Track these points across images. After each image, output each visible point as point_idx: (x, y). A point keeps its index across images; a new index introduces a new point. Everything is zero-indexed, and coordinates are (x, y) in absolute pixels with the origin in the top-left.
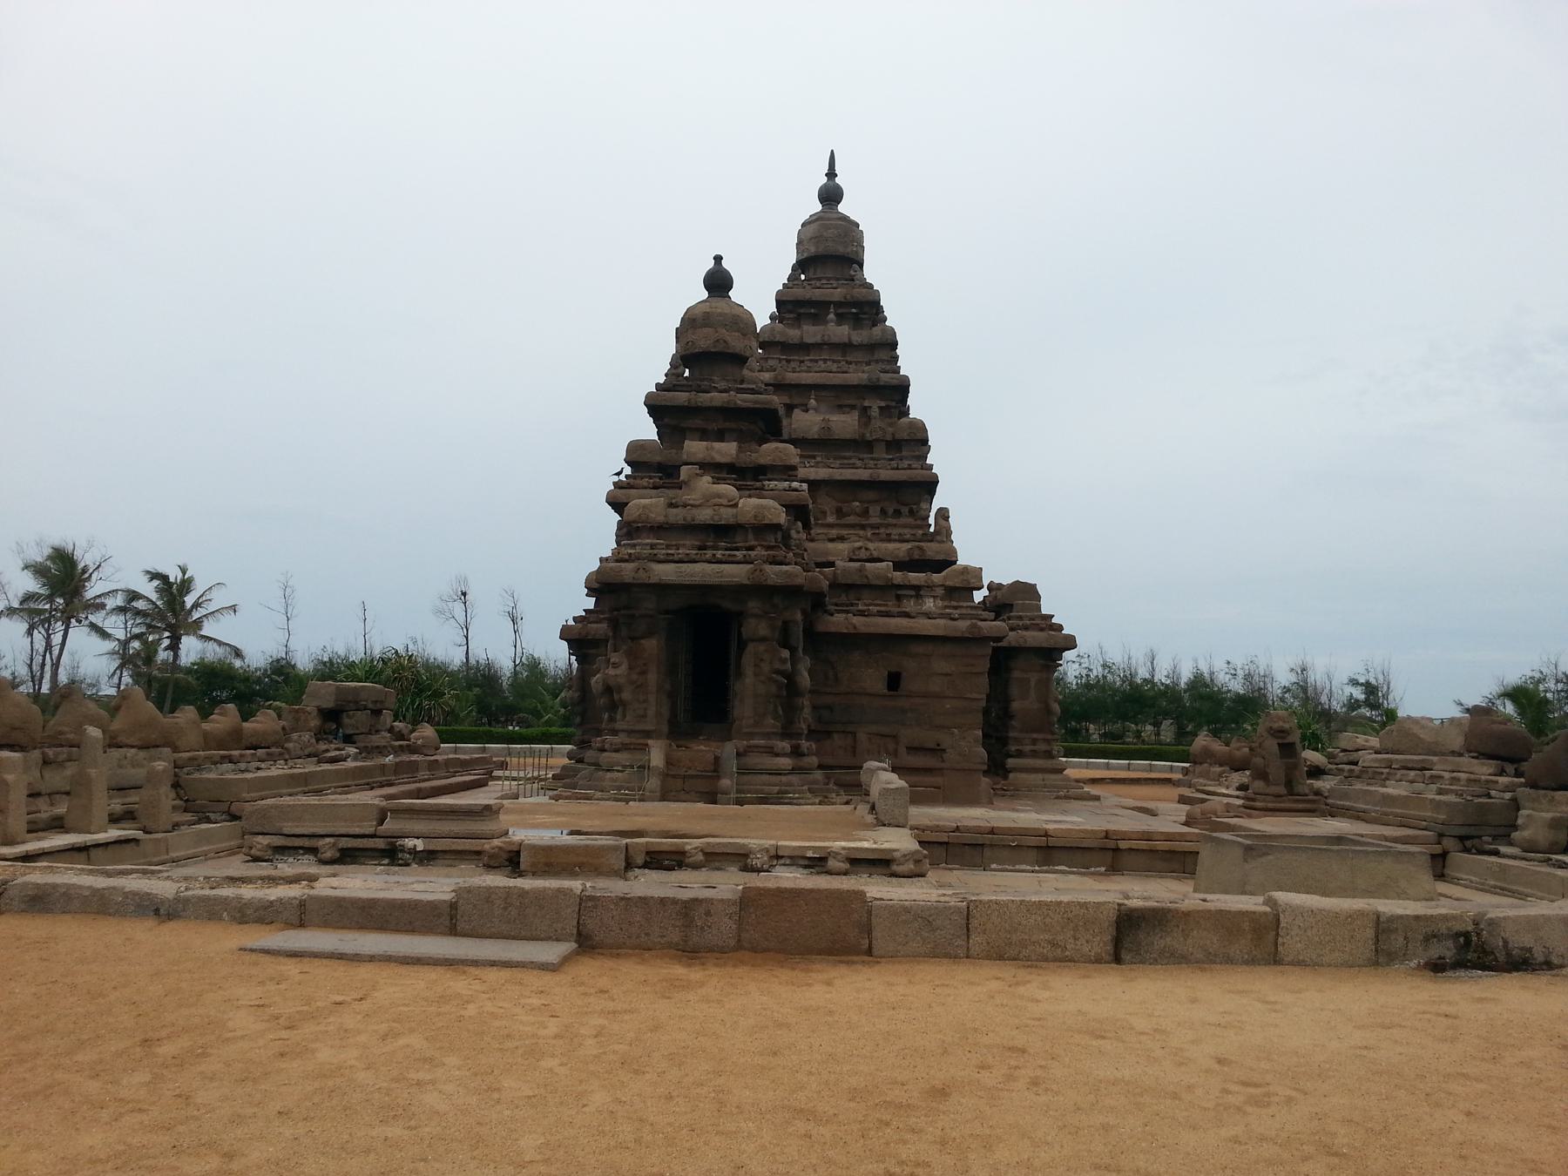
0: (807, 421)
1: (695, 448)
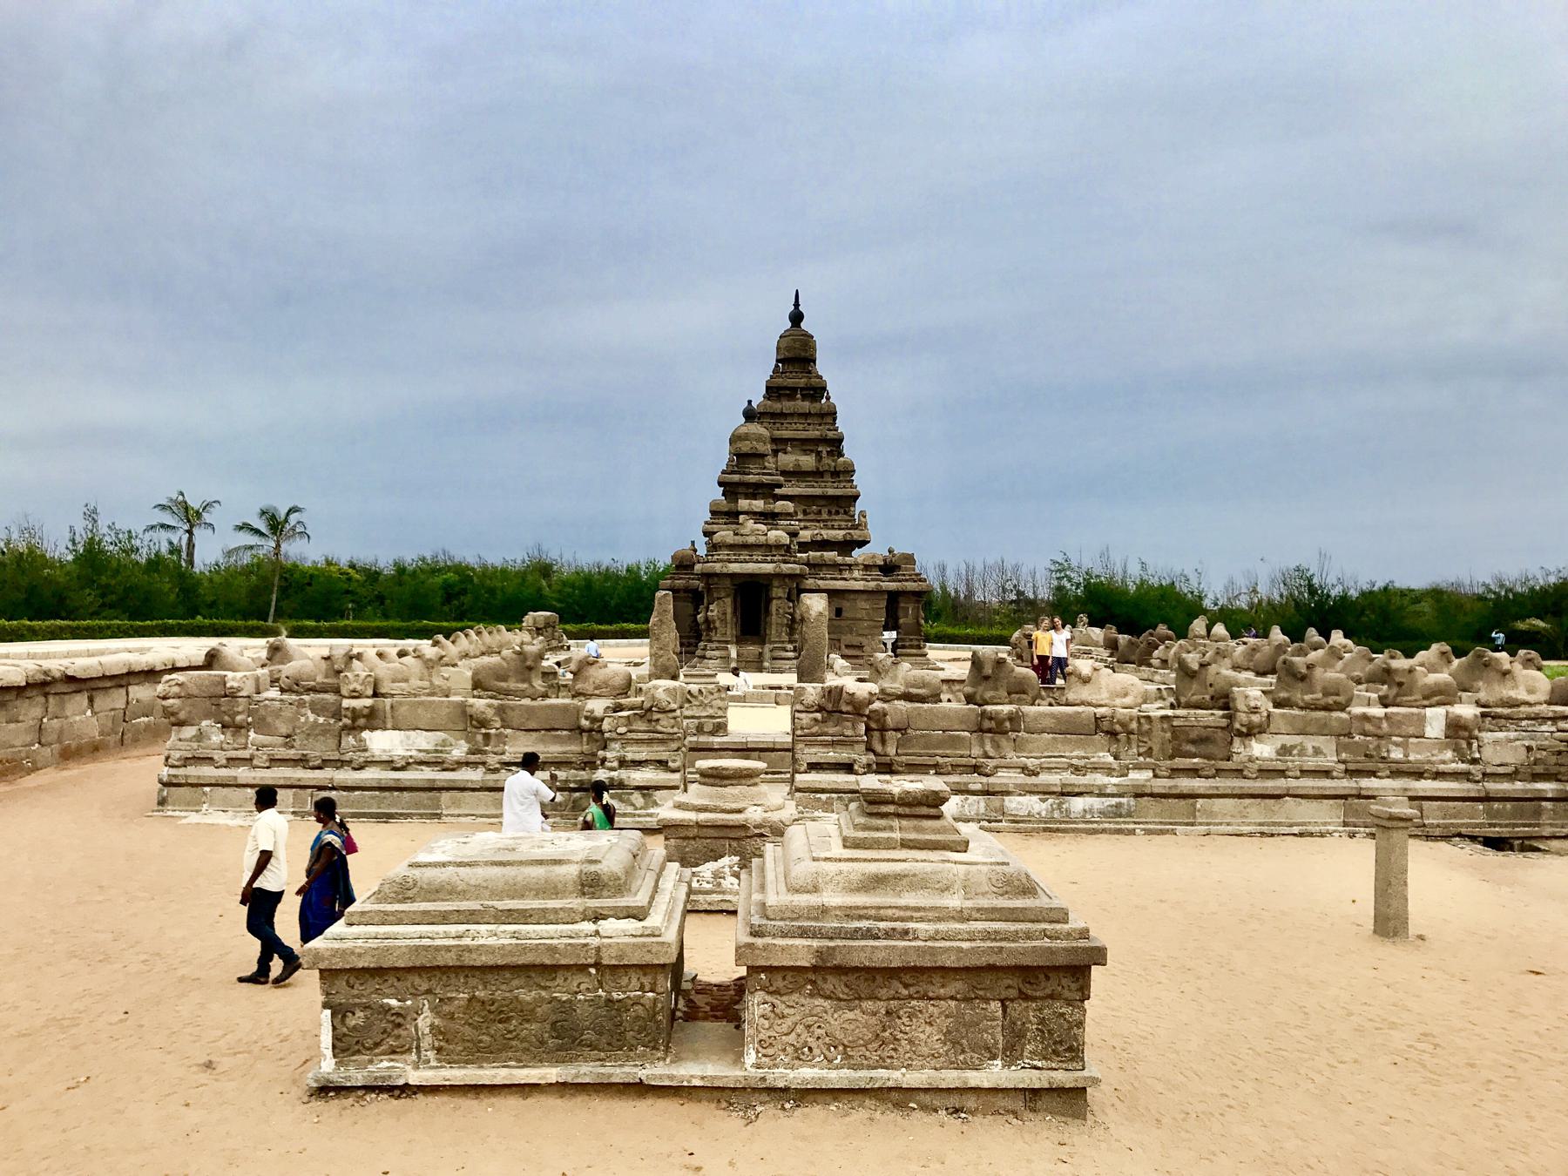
0: (788, 460)
1: (743, 504)
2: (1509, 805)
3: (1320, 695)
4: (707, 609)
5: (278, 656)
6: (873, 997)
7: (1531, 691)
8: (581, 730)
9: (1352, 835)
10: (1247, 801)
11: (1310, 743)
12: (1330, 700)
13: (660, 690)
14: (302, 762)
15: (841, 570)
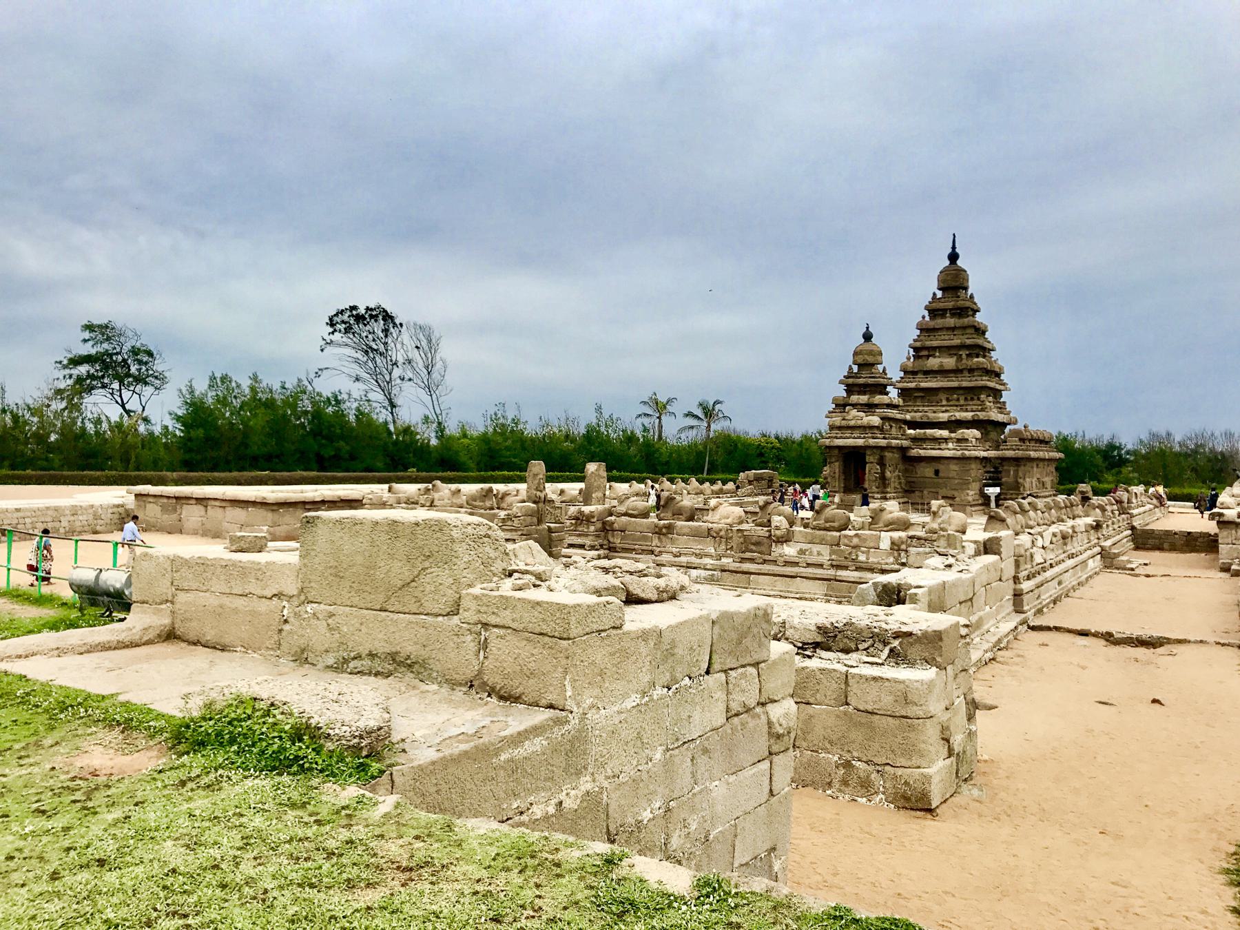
1: (855, 398)
9: (828, 601)
11: (816, 548)
12: (828, 525)
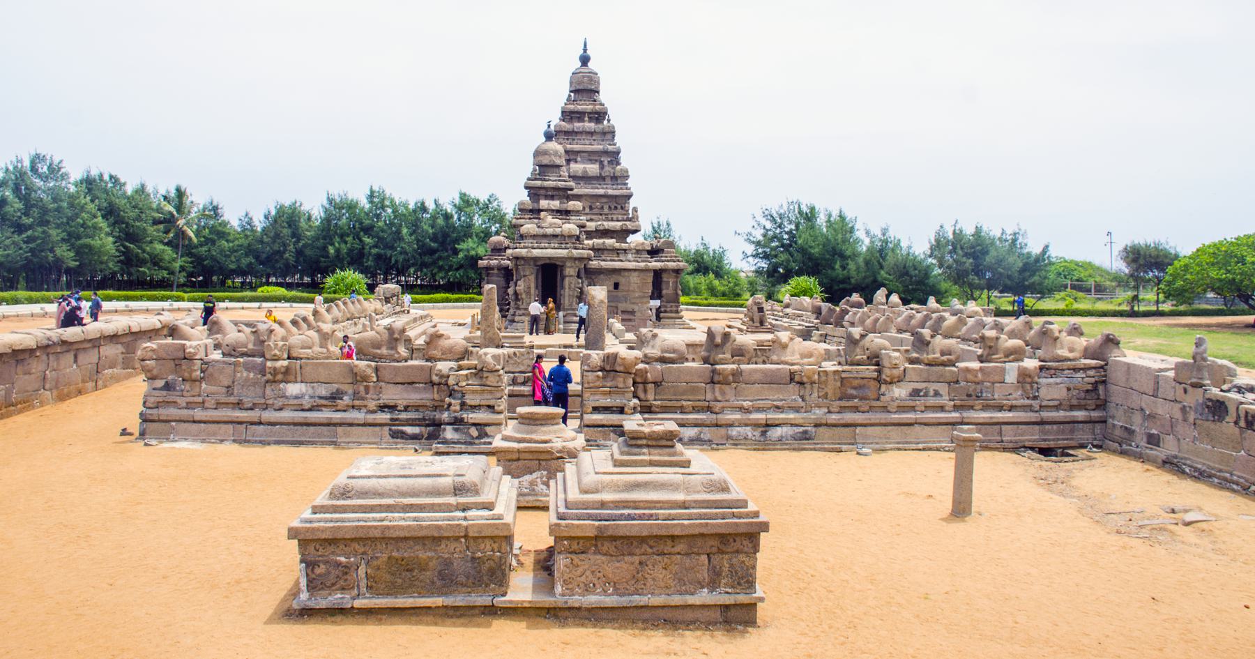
0: (577, 168)
1: (544, 203)
2: (1055, 427)
3: (938, 355)
4: (516, 285)
5: (215, 328)
6: (631, 554)
7: (1071, 350)
8: (433, 384)
10: (890, 428)
12: (945, 358)
13: (489, 356)
14: (239, 405)
15: (618, 254)
